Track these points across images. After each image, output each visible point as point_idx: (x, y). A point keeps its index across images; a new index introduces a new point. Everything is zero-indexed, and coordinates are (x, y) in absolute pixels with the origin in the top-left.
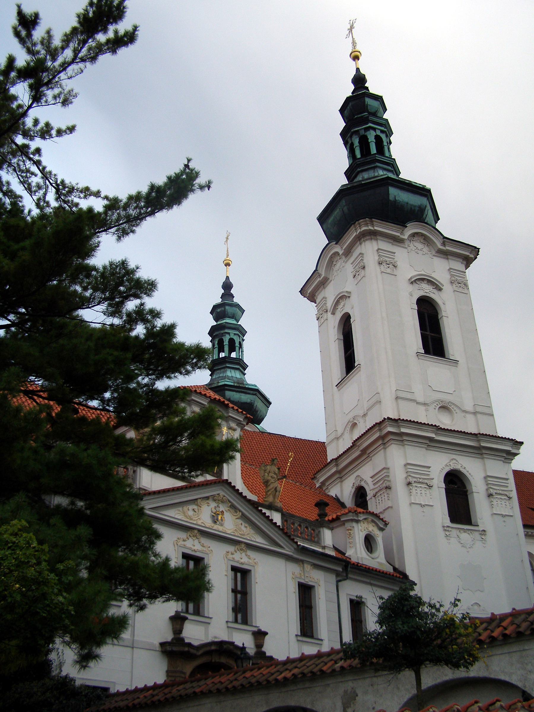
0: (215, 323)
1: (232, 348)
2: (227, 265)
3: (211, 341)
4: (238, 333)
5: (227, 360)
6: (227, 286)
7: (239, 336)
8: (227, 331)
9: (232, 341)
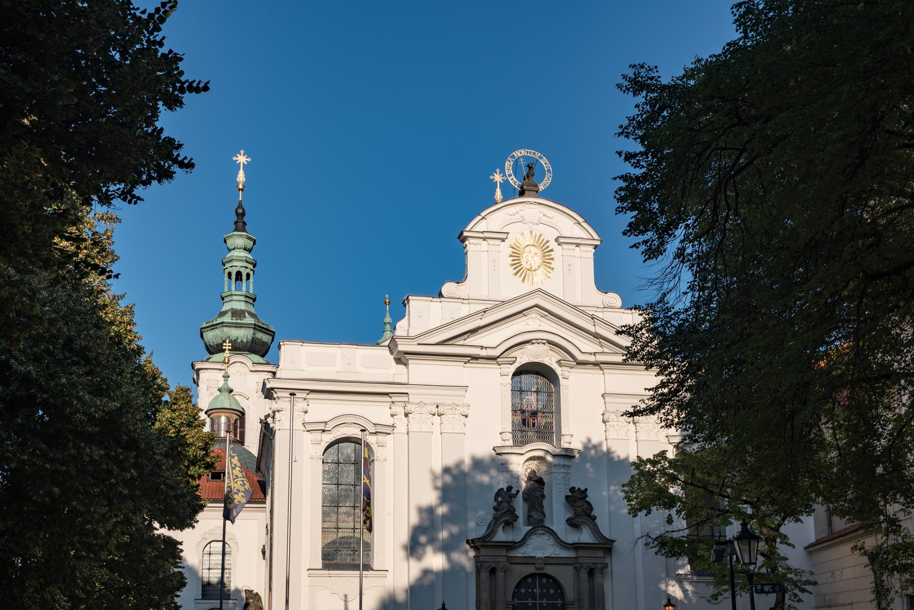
8: (235, 263)
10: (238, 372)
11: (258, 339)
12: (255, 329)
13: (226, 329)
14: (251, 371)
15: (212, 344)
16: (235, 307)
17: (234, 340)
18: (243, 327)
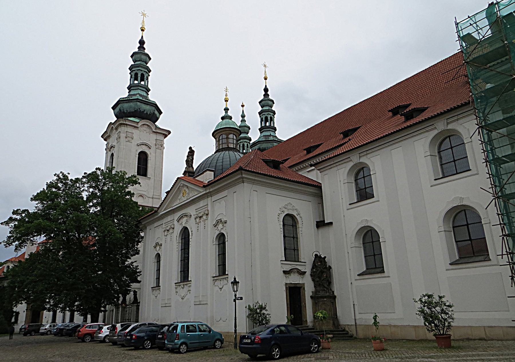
0: (133, 63)
1: (142, 80)
2: (143, 30)
3: (130, 73)
4: (146, 71)
5: (138, 85)
6: (142, 42)
7: (147, 73)
9: (142, 75)
10: (145, 131)
11: (155, 114)
12: (155, 108)
13: (138, 103)
14: (154, 132)
15: (125, 112)
16: (140, 93)
17: (142, 111)
18: (149, 105)
